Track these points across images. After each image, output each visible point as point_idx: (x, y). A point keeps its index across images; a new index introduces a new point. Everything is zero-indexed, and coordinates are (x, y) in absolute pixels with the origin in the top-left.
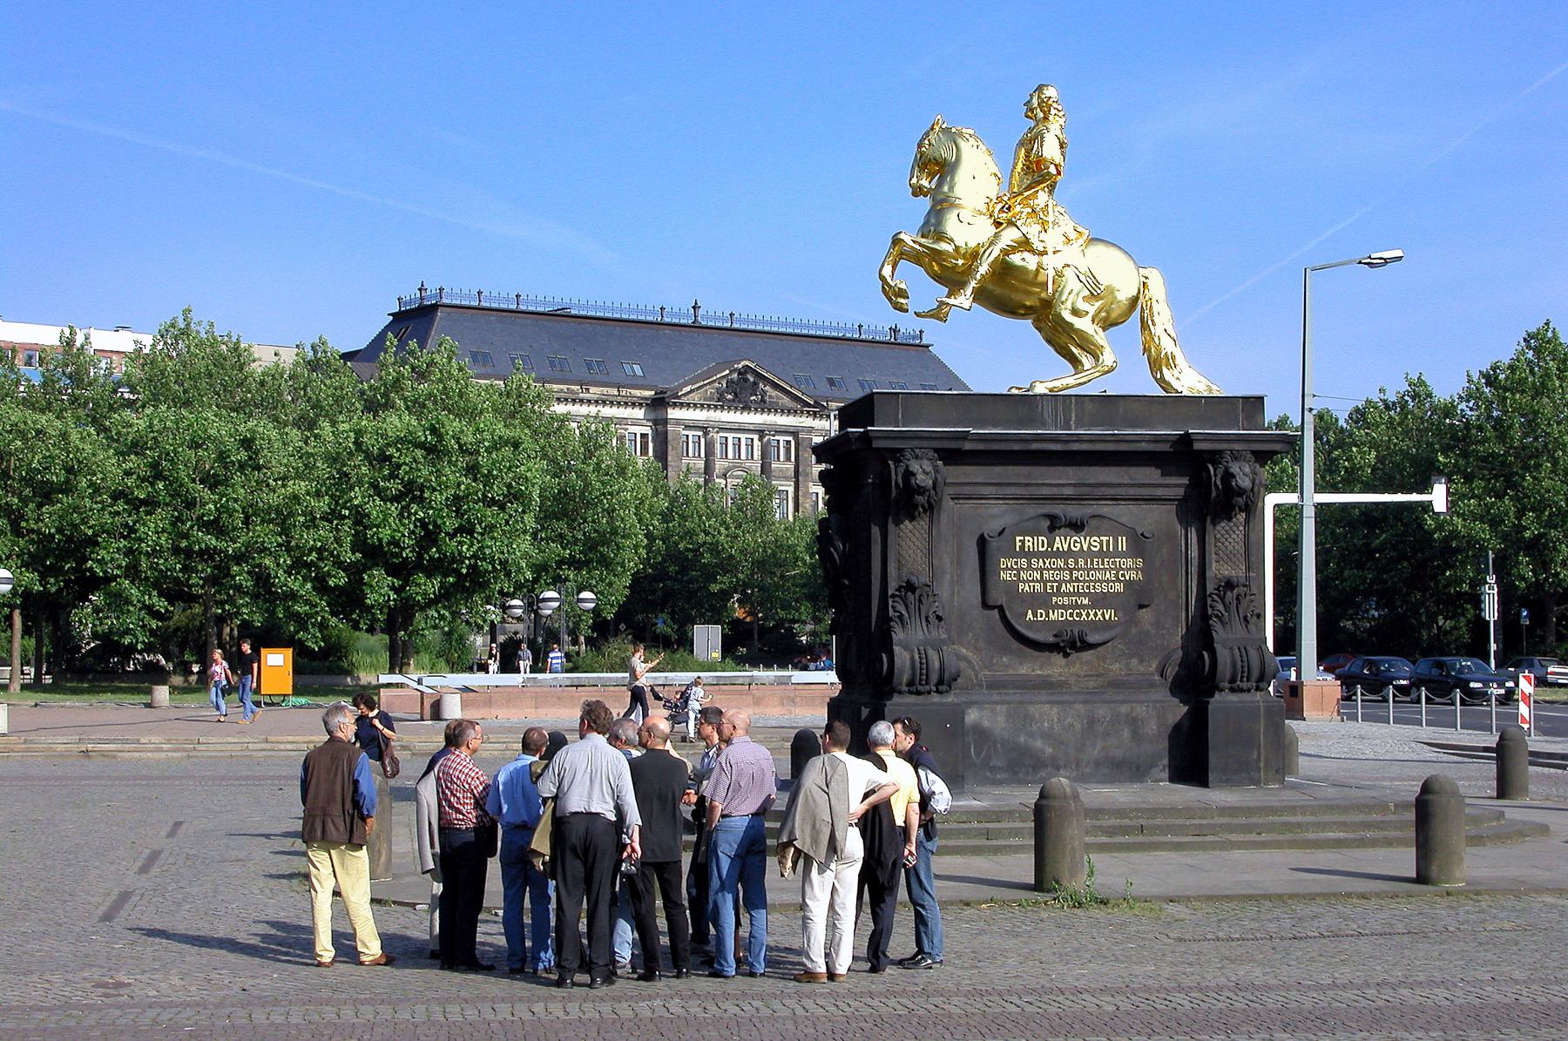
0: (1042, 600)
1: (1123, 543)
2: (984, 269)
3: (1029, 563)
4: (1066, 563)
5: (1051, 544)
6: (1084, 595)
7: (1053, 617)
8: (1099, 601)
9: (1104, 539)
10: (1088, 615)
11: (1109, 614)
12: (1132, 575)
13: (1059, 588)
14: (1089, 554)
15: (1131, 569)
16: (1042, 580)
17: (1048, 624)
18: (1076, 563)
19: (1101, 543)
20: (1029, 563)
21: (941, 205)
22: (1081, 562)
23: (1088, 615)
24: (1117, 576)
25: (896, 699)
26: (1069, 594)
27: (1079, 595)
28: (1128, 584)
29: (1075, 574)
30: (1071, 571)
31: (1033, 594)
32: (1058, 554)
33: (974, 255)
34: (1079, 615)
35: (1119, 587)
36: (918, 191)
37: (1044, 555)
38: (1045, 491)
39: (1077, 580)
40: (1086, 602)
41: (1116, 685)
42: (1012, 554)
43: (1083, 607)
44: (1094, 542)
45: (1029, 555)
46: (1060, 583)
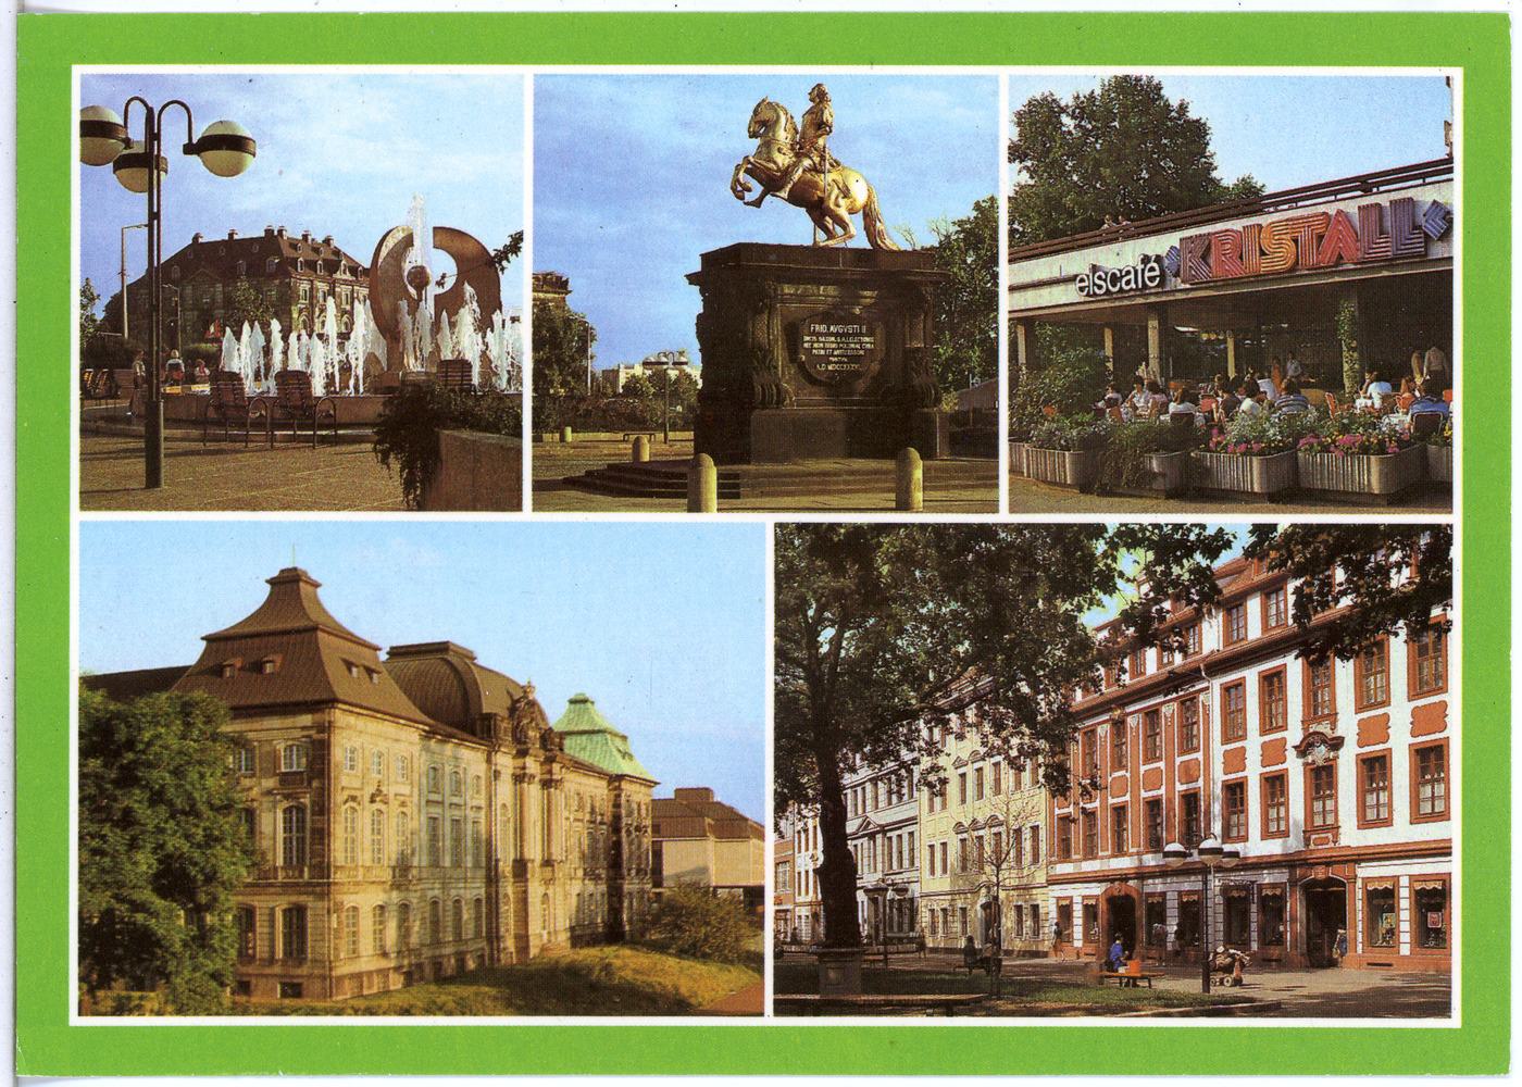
0: (826, 359)
7: (830, 368)
21: (768, 145)
25: (757, 412)
27: (842, 356)
32: (832, 334)
35: (862, 352)
36: (753, 135)
37: (826, 335)
42: (811, 334)
45: (819, 334)
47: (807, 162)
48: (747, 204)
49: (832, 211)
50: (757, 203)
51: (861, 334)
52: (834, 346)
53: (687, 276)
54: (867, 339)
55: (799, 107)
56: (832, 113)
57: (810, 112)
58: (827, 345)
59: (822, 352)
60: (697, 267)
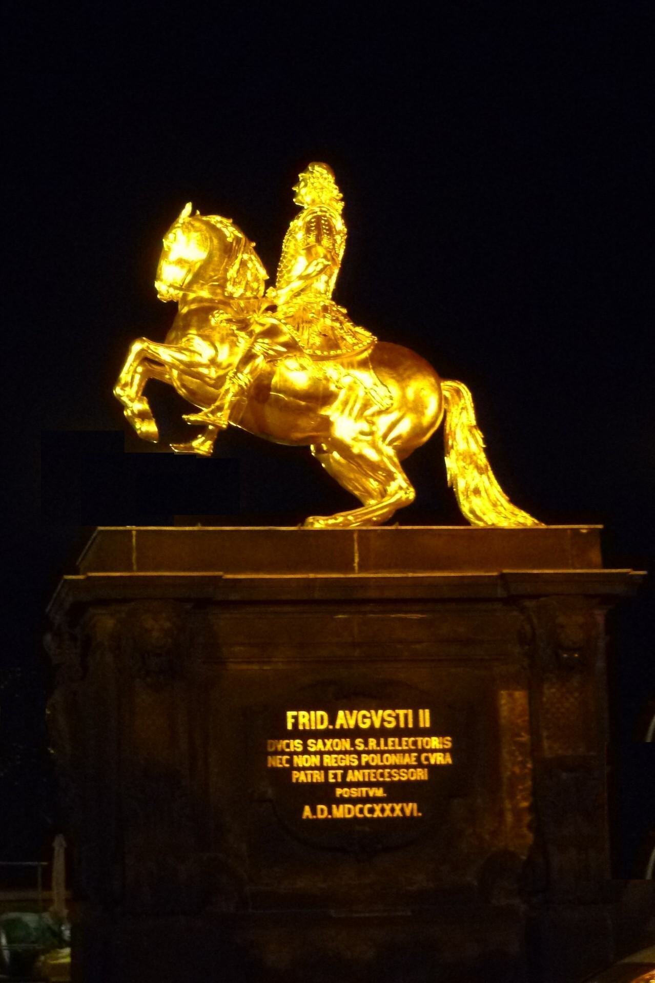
0: (323, 793)
1: (425, 718)
3: (305, 745)
4: (353, 744)
5: (332, 720)
6: (377, 784)
8: (397, 791)
9: (401, 712)
10: (383, 810)
11: (411, 808)
12: (438, 759)
13: (344, 776)
14: (381, 733)
15: (438, 750)
16: (325, 769)
18: (366, 744)
19: (397, 718)
20: (305, 745)
22: (372, 742)
23: (383, 810)
24: (418, 759)
26: (358, 784)
27: (370, 784)
28: (434, 769)
29: (365, 758)
30: (359, 753)
31: (312, 786)
34: (371, 811)
35: (421, 775)
40: (379, 792)
43: (376, 800)
46: (346, 769)
52: (352, 760)
54: (435, 742)
58: (329, 760)
59: (318, 777)
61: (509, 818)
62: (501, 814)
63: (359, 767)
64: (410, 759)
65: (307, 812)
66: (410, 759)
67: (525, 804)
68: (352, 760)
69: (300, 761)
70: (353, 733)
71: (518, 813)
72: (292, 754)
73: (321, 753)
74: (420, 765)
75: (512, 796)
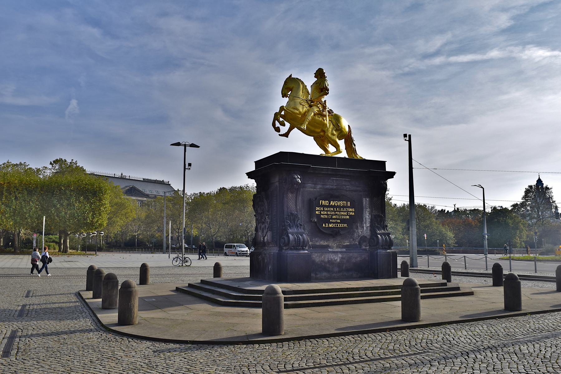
0: (327, 221)
1: (349, 203)
2: (310, 118)
5: (330, 203)
7: (330, 226)
8: (343, 221)
17: (329, 227)
28: (350, 216)
32: (332, 206)
33: (305, 115)
35: (348, 217)
38: (328, 187)
39: (337, 215)
41: (346, 247)
43: (339, 223)
44: (341, 203)
45: (324, 206)
47: (316, 110)
48: (280, 135)
49: (330, 138)
50: (286, 135)
51: (347, 207)
52: (333, 213)
53: (247, 174)
54: (351, 210)
55: (309, 81)
56: (330, 83)
57: (315, 83)
59: (326, 216)
60: (252, 168)
61: (365, 228)
62: (363, 227)
63: (335, 215)
64: (345, 214)
65: (324, 225)
66: (345, 214)
67: (368, 225)
68: (333, 213)
69: (322, 213)
70: (333, 207)
71: (367, 228)
72: (321, 211)
73: (327, 211)
74: (347, 215)
75: (366, 223)
